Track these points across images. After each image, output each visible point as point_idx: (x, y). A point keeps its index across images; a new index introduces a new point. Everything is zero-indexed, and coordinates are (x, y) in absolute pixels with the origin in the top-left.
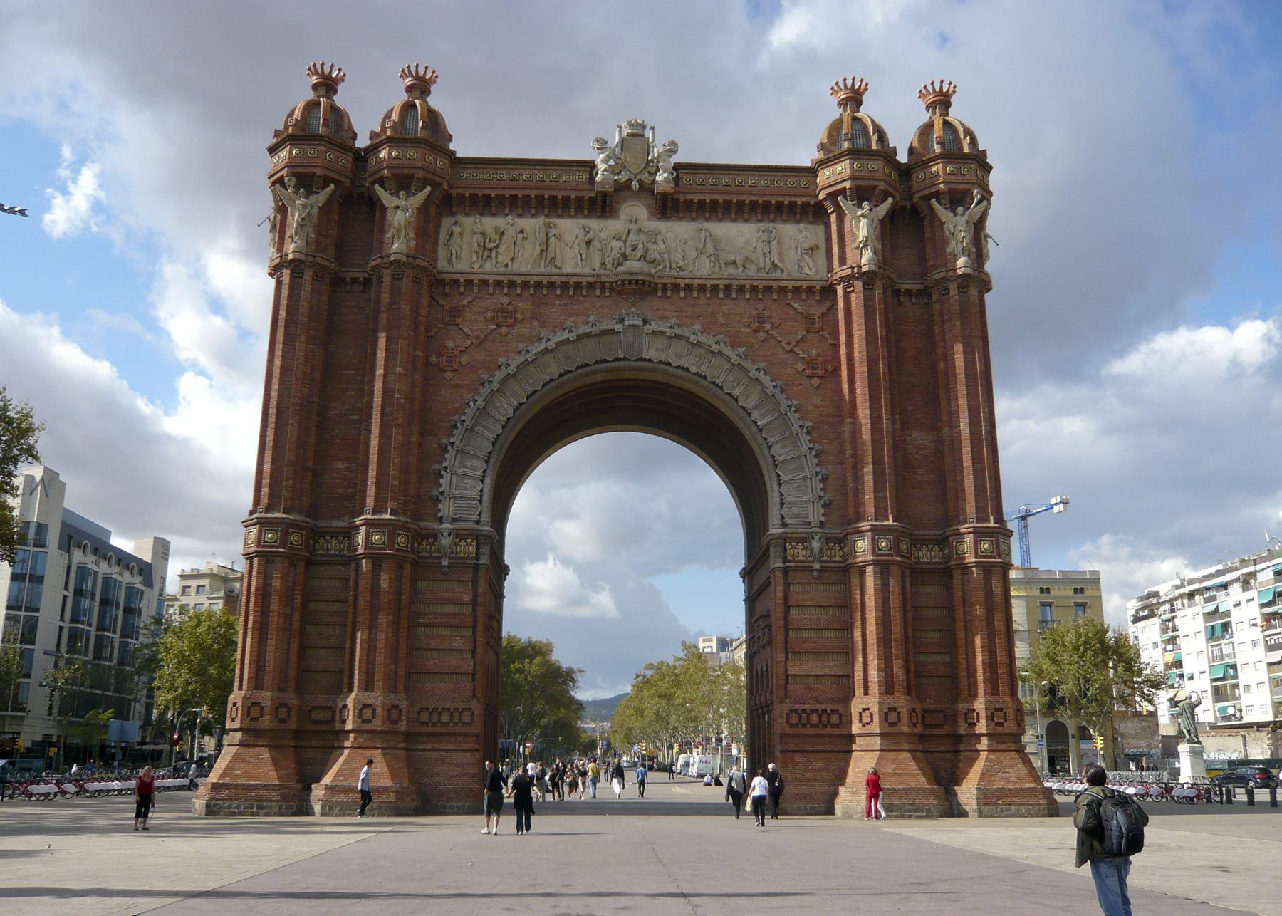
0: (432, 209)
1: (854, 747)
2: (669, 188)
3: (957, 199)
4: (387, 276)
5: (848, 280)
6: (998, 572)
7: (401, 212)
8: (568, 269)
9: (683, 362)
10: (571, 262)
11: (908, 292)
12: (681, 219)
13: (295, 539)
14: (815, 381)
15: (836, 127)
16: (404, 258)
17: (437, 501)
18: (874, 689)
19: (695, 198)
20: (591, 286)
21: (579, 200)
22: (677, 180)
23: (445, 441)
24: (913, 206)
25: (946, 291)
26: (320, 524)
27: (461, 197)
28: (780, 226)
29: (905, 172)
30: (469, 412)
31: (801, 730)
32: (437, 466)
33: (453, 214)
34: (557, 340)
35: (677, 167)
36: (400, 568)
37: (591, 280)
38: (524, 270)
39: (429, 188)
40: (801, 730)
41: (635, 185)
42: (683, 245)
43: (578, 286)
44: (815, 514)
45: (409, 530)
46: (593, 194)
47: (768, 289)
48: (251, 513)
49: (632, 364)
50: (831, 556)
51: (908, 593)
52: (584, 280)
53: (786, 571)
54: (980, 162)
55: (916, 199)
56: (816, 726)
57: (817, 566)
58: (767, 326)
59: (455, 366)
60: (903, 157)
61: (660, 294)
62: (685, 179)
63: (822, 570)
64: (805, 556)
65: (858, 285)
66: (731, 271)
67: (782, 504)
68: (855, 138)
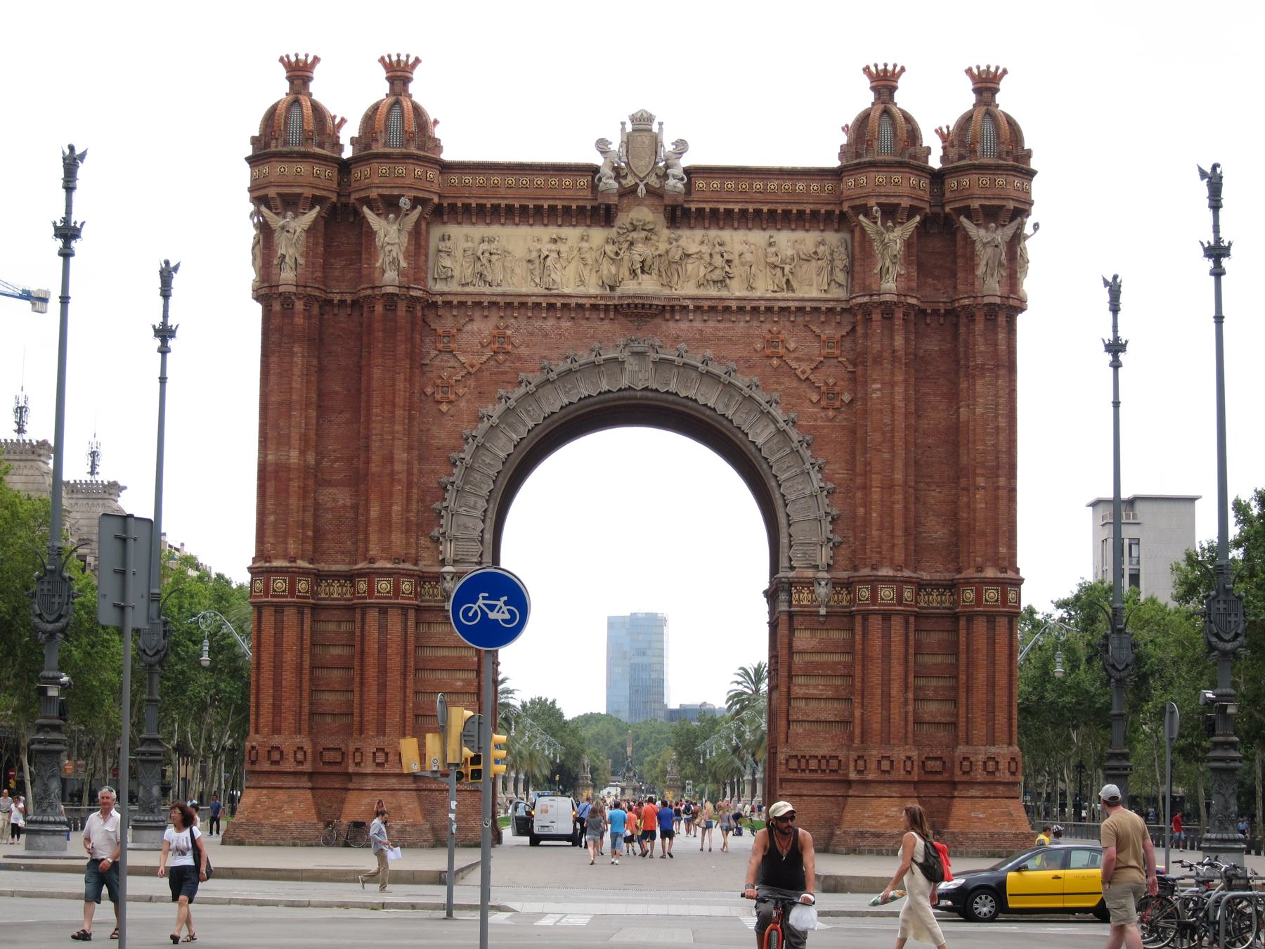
0: (423, 226)
1: (851, 792)
4: (379, 308)
6: (1002, 623)
7: (389, 234)
9: (692, 394)
11: (936, 312)
12: (691, 228)
13: (302, 586)
14: (831, 413)
15: (864, 118)
16: (396, 291)
17: (437, 541)
19: (707, 207)
20: (595, 307)
21: (581, 209)
22: (689, 186)
23: (445, 479)
24: (947, 216)
25: (972, 318)
26: (323, 566)
27: (453, 207)
29: (937, 178)
30: (469, 448)
31: (799, 775)
32: (437, 505)
33: (444, 223)
34: (557, 370)
35: (690, 172)
36: (405, 615)
37: (592, 301)
39: (419, 208)
40: (799, 775)
41: (642, 190)
43: (580, 307)
44: (824, 556)
45: (411, 576)
46: (595, 203)
48: (254, 560)
49: (639, 394)
50: (838, 601)
51: (912, 643)
52: (587, 302)
53: (791, 615)
55: (947, 209)
56: (815, 771)
57: (823, 611)
58: (781, 351)
59: (452, 397)
60: (935, 162)
61: (668, 316)
62: (700, 183)
63: (828, 615)
64: (812, 601)
65: (876, 316)
67: (791, 546)
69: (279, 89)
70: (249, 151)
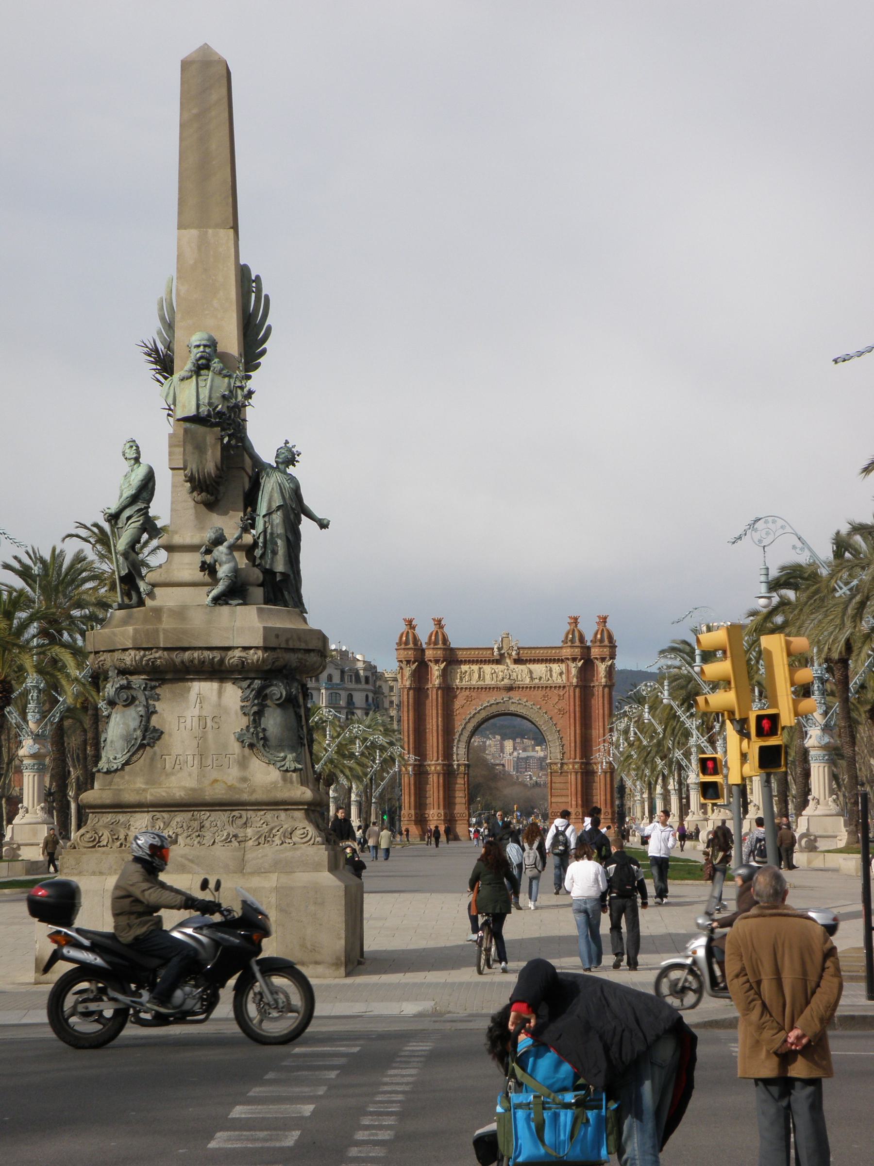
2: (516, 657)
3: (603, 660)
5: (569, 686)
8: (486, 683)
10: (488, 681)
18: (574, 806)
28: (551, 665)
35: (518, 648)
38: (474, 683)
42: (521, 672)
44: (559, 756)
47: (546, 687)
54: (613, 647)
65: (572, 688)
66: (537, 681)
68: (575, 636)
69: (403, 628)
70: (396, 647)
